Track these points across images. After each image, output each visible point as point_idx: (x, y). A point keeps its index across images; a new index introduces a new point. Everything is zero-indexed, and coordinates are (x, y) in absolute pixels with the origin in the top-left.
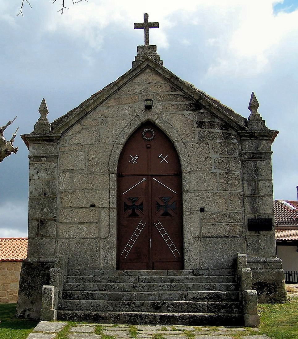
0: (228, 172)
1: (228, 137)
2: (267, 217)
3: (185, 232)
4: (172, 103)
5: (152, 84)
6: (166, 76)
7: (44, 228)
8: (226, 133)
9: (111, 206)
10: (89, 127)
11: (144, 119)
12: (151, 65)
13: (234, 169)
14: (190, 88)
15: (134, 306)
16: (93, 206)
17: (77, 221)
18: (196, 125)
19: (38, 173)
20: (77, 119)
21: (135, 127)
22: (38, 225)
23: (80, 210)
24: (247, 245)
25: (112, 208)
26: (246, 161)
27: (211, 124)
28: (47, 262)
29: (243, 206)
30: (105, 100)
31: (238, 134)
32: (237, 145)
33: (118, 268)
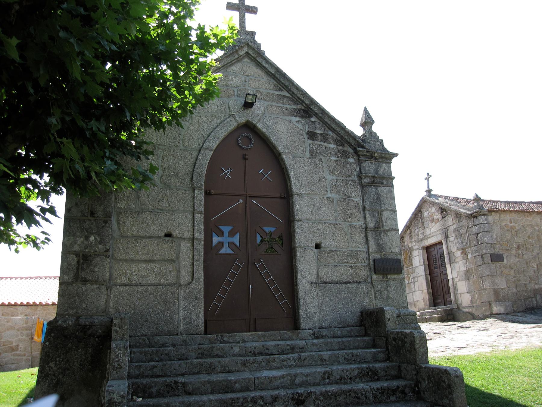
1: (343, 155)
2: (394, 257)
4: (277, 105)
5: (252, 78)
6: (270, 70)
7: (88, 267)
8: (341, 150)
9: (196, 236)
11: (242, 118)
12: (251, 52)
13: (353, 195)
15: (262, 404)
16: (168, 235)
17: (144, 257)
18: (306, 136)
22: (78, 262)
23: (148, 241)
24: (375, 293)
25: (197, 239)
26: (366, 186)
27: (323, 136)
29: (367, 242)
32: (355, 166)
33: (206, 332)
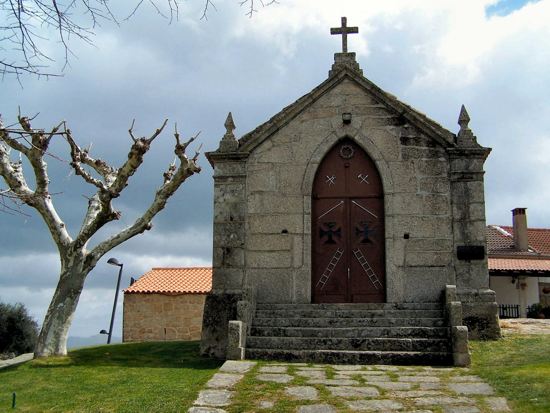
0: (435, 194)
2: (479, 245)
3: (387, 261)
4: (373, 117)
6: (366, 87)
7: (230, 256)
8: (433, 150)
9: (305, 232)
10: (281, 144)
11: (342, 134)
13: (442, 190)
14: (393, 100)
16: (285, 232)
17: (268, 249)
18: (399, 142)
19: (223, 195)
20: (267, 135)
21: (331, 143)
23: (270, 236)
24: (457, 276)
25: (306, 234)
26: (455, 182)
28: (234, 295)
29: (453, 232)
30: (298, 114)
31: (447, 151)
32: (445, 164)
33: (313, 302)
